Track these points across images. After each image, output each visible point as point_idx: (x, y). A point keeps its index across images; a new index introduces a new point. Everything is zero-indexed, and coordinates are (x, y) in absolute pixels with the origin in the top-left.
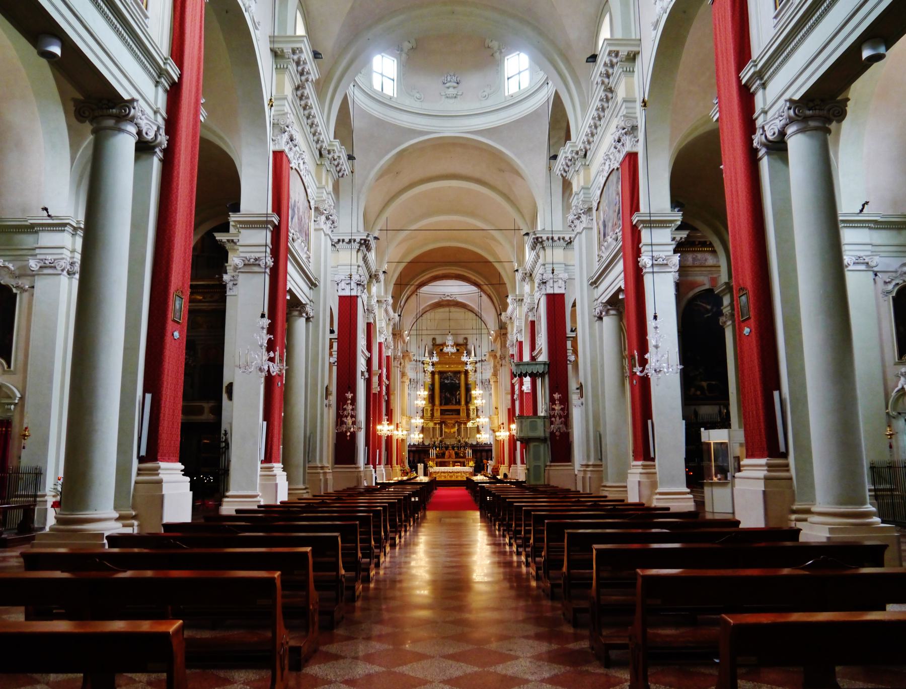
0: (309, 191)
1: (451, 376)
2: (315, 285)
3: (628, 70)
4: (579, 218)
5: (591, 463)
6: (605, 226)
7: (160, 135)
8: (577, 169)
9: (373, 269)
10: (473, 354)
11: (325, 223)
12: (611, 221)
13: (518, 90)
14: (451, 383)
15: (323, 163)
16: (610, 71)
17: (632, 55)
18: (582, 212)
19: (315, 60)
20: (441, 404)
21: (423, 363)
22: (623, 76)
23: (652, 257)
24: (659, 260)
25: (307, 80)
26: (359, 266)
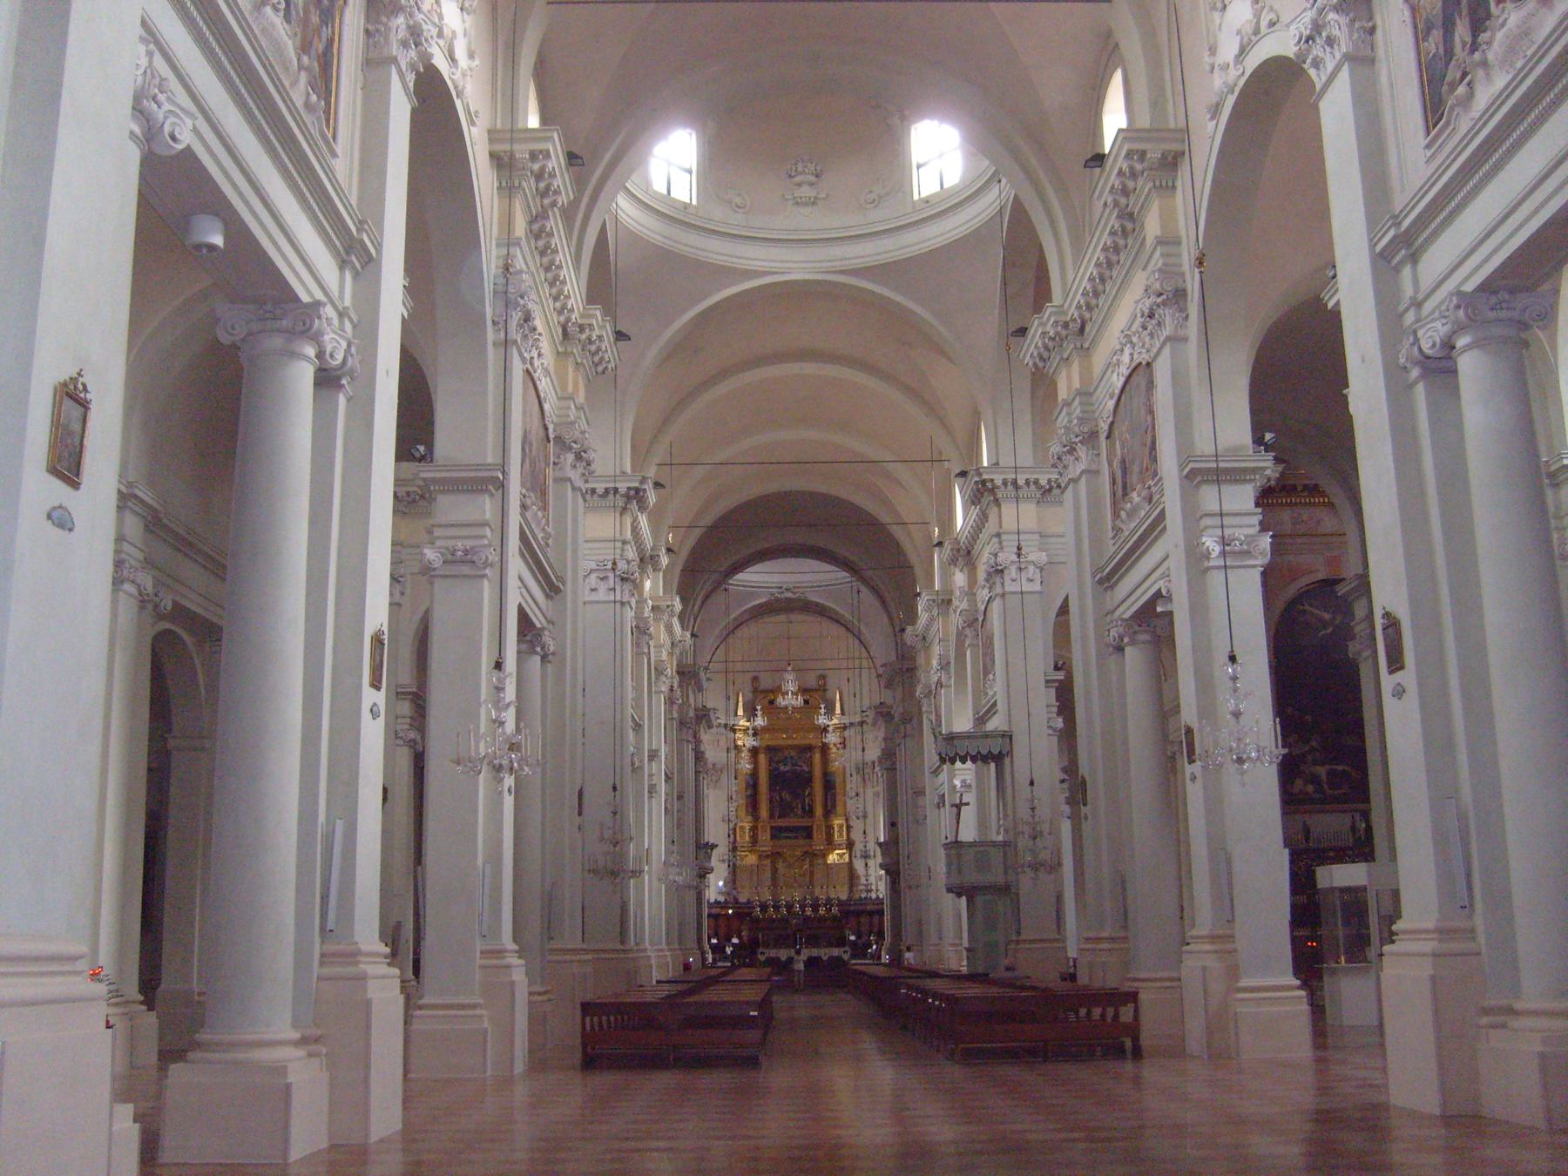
0: (546, 407)
1: (792, 758)
2: (557, 590)
3: (1164, 183)
4: (1072, 451)
5: (1105, 934)
6: (1125, 471)
7: (352, 355)
8: (1065, 356)
9: (649, 542)
10: (838, 711)
11: (575, 466)
12: (1137, 462)
13: (938, 189)
15: (569, 350)
16: (1130, 184)
17: (1170, 158)
18: (1077, 440)
19: (571, 168)
20: (772, 816)
21: (734, 731)
22: (1153, 190)
23: (1223, 537)
24: (1233, 544)
25: (554, 204)
26: (624, 542)
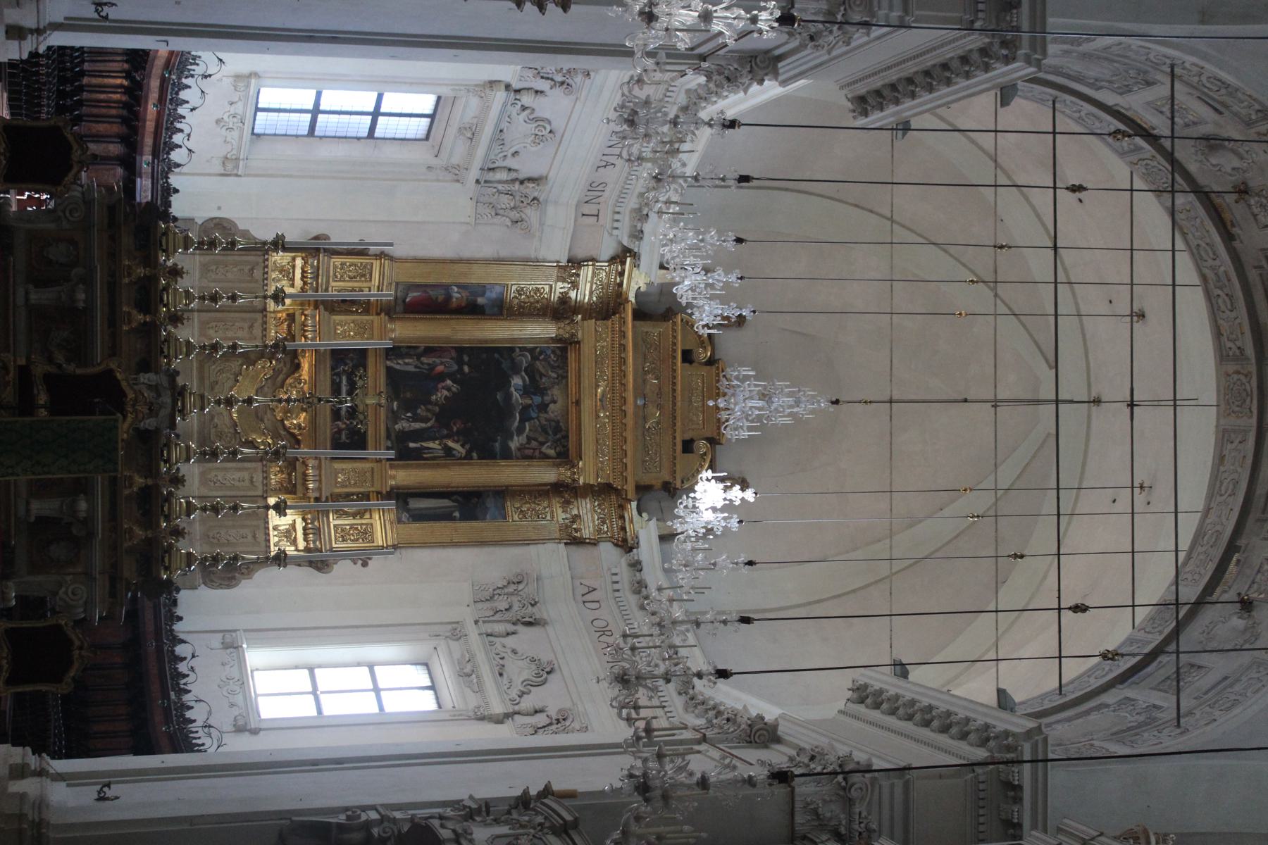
1: (543, 407)
14: (505, 410)
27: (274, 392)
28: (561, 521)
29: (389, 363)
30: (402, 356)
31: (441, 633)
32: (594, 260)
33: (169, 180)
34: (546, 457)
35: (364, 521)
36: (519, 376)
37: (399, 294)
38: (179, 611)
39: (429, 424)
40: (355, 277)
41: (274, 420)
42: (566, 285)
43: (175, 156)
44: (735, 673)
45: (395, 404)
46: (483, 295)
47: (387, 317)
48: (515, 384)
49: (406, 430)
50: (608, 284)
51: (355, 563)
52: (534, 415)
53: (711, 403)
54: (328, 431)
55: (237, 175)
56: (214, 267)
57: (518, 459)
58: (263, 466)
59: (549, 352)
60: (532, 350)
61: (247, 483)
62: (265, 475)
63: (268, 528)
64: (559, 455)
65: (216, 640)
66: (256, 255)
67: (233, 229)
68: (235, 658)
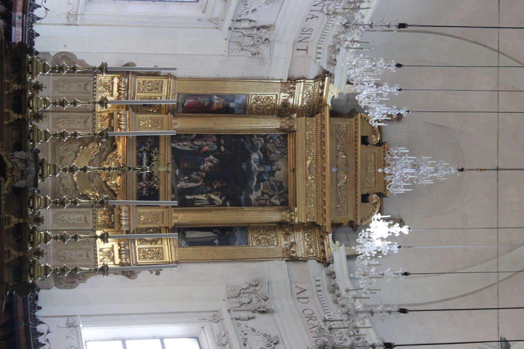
1: (272, 173)
27: (100, 163)
28: (283, 246)
29: (173, 145)
30: (181, 140)
31: (206, 318)
32: (304, 78)
33: (33, 28)
34: (274, 205)
35: (157, 246)
36: (256, 153)
37: (180, 101)
38: (39, 303)
39: (199, 184)
40: (151, 90)
41: (100, 181)
42: (287, 95)
43: (37, 12)
44: (397, 346)
45: (177, 171)
46: (233, 101)
47: (172, 115)
48: (254, 158)
49: (184, 187)
50: (314, 95)
51: (152, 273)
52: (266, 178)
53: (380, 170)
54: (135, 188)
55: (76, 25)
56: (62, 84)
57: (256, 206)
58: (93, 210)
59: (275, 138)
60: (264, 137)
61: (83, 221)
62: (94, 216)
63: (96, 250)
64: (282, 204)
65: (63, 322)
66: (88, 76)
67: (74, 59)
68: (75, 333)
